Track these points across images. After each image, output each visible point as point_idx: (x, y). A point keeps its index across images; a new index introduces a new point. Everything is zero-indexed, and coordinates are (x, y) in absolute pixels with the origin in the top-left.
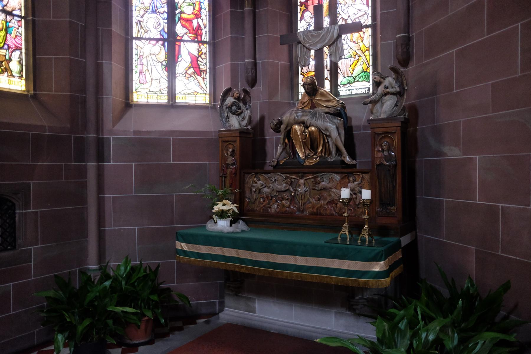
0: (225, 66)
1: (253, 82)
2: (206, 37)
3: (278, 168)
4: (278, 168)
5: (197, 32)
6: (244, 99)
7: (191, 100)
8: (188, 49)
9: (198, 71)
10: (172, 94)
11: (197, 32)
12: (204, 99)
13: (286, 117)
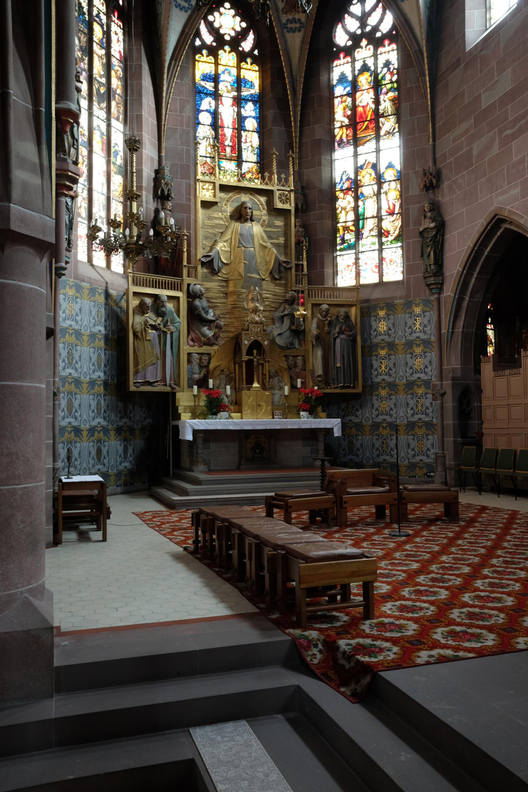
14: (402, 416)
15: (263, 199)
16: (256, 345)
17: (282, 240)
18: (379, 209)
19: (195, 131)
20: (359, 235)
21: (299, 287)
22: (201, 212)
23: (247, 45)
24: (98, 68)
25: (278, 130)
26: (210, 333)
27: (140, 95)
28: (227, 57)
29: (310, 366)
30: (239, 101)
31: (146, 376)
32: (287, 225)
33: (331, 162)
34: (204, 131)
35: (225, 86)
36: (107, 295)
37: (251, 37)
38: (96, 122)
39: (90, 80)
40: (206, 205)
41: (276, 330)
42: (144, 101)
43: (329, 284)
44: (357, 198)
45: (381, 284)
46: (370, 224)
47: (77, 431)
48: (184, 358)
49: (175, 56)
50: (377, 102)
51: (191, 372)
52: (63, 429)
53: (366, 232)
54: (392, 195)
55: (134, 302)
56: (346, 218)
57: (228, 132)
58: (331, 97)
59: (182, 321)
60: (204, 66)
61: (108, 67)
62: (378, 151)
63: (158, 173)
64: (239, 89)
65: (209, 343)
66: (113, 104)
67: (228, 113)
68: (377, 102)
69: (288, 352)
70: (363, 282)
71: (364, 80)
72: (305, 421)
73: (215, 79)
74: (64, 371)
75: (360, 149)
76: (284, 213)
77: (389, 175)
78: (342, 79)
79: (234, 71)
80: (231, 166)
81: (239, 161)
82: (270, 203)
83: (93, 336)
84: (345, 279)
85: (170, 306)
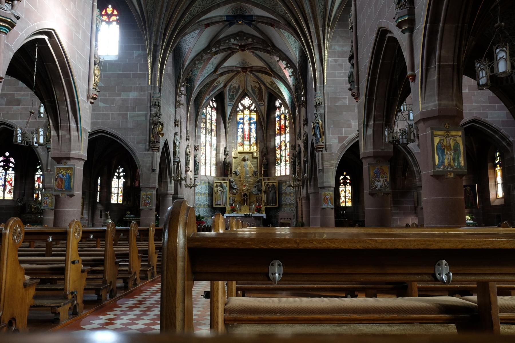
1: (24, 196)
2: (13, 185)
6: (22, 200)
7: (8, 198)
8: (8, 188)
10: (4, 197)
11: (11, 184)
12: (11, 198)
13: (31, 204)
15: (251, 155)
16: (245, 195)
17: (256, 165)
18: (285, 154)
19: (237, 134)
20: (281, 162)
21: (261, 178)
23: (252, 108)
24: (208, 125)
25: (260, 132)
26: (235, 191)
27: (220, 129)
28: (247, 112)
29: (263, 200)
30: (250, 124)
31: (218, 203)
32: (257, 161)
33: (274, 140)
34: (240, 134)
36: (209, 183)
37: (254, 105)
40: (235, 158)
41: (253, 190)
43: (273, 176)
44: (281, 150)
45: (286, 175)
46: (284, 158)
49: (229, 117)
50: (285, 123)
51: (230, 202)
53: (283, 160)
54: (288, 151)
55: (215, 185)
56: (278, 156)
58: (275, 121)
59: (228, 189)
60: (240, 115)
61: (211, 124)
62: (285, 137)
64: (250, 121)
65: (235, 194)
66: (213, 133)
68: (285, 123)
70: (282, 175)
71: (283, 116)
72: (256, 214)
73: (243, 119)
74: (196, 202)
75: (282, 136)
76: (256, 158)
78: (278, 116)
79: (249, 116)
81: (250, 141)
82: (253, 155)
85: (225, 185)
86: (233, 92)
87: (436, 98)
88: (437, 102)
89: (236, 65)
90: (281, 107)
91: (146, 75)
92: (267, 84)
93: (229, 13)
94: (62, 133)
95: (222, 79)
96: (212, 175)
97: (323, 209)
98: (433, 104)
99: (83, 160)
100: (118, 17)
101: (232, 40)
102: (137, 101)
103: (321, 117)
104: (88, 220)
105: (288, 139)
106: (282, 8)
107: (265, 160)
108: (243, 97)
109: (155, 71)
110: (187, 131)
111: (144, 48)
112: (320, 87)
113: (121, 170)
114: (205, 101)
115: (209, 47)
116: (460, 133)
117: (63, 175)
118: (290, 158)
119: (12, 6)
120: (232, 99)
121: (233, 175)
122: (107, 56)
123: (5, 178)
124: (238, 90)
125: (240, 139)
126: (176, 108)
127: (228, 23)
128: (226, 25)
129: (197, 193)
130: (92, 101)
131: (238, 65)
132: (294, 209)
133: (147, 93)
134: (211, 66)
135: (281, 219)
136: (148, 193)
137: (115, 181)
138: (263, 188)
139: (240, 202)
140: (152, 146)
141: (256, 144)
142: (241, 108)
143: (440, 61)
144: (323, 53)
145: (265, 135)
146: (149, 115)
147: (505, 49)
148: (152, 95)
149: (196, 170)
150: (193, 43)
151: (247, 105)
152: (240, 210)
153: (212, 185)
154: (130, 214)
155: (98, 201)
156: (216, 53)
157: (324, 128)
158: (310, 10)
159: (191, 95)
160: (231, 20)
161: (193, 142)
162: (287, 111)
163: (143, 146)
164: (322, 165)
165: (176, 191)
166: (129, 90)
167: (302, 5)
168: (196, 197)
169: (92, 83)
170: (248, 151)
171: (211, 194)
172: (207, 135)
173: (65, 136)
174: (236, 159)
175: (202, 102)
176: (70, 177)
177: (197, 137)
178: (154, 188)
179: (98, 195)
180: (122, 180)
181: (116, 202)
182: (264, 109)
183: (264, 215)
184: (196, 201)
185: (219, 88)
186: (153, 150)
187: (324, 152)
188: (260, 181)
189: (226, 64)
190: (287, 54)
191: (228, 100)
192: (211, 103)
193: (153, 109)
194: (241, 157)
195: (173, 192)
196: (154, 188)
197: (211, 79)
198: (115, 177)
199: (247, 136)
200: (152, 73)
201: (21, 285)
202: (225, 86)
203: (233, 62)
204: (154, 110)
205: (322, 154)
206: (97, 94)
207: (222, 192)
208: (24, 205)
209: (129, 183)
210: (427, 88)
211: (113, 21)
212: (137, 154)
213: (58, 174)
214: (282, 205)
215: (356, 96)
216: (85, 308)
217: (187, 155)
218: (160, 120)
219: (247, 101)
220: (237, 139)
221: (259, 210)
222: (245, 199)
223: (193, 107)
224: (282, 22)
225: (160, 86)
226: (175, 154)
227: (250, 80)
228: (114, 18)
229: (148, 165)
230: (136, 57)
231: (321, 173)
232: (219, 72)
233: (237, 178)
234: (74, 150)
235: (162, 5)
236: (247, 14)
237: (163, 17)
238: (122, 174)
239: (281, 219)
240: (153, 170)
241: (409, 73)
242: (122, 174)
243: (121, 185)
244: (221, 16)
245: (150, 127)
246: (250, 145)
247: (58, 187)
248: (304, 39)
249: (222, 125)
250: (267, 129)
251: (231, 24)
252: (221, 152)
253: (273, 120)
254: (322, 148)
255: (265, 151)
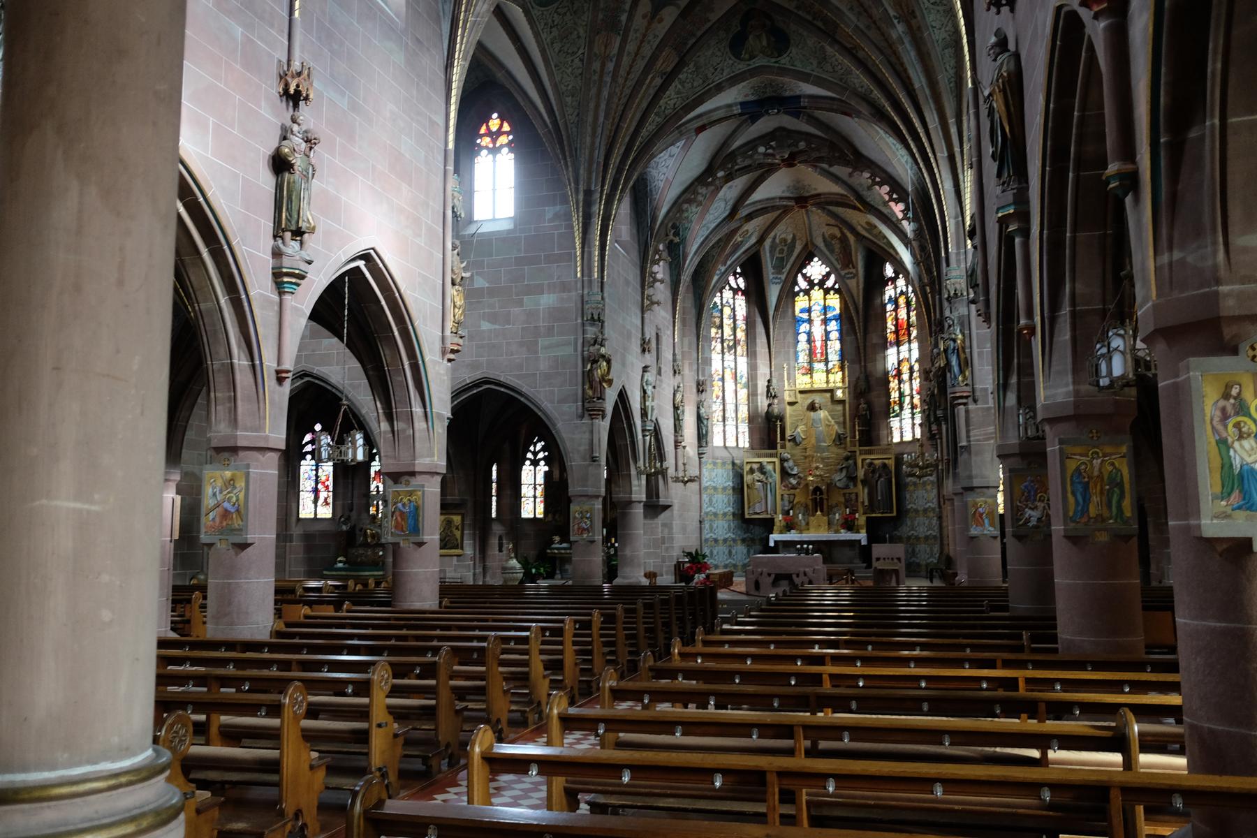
0: (339, 503)
1: (351, 510)
2: (331, 488)
3: (361, 545)
4: (361, 545)
5: (327, 487)
8: (323, 495)
9: (327, 504)
11: (327, 487)
12: (330, 516)
14: (922, 531)
15: (828, 395)
16: (817, 489)
17: (841, 419)
18: (912, 390)
20: (901, 408)
21: (853, 449)
22: (788, 408)
24: (728, 331)
26: (794, 481)
28: (817, 294)
29: (860, 500)
30: (825, 322)
31: (756, 509)
33: (885, 358)
34: (803, 345)
35: (817, 316)
36: (733, 464)
37: (833, 278)
38: (726, 364)
39: (722, 342)
40: (791, 404)
41: (837, 477)
42: (758, 341)
44: (900, 382)
46: (907, 399)
47: (716, 541)
48: (778, 497)
49: (776, 309)
50: (909, 317)
51: (783, 506)
52: (707, 540)
54: (916, 384)
55: (747, 468)
56: (895, 395)
57: (818, 344)
59: (777, 476)
60: (801, 302)
61: (734, 329)
62: (910, 350)
63: (769, 381)
66: (739, 348)
67: (818, 331)
68: (909, 317)
69: (848, 491)
70: (905, 439)
71: (902, 300)
72: (845, 535)
73: (809, 310)
74: (706, 508)
76: (842, 402)
77: (916, 367)
80: (821, 366)
81: (827, 361)
82: (832, 397)
83: (724, 489)
84: (896, 439)
85: (770, 467)
86: (782, 251)
87: (1070, 379)
88: (1071, 388)
89: (779, 194)
90: (897, 277)
91: (571, 257)
92: (859, 229)
93: (747, 95)
94: (399, 425)
95: (753, 227)
96: (741, 445)
97: (972, 538)
98: (1064, 390)
99: (438, 474)
100: (511, 137)
101: (762, 149)
102: (556, 314)
103: (962, 325)
104: (474, 558)
105: (915, 354)
106: (860, 80)
107: (863, 406)
108: (807, 259)
109: (589, 247)
110: (674, 355)
111: (565, 201)
112: (958, 254)
113: (539, 446)
114: (716, 278)
115: (709, 171)
116: (1124, 449)
117: (404, 505)
118: (922, 401)
119: (301, 243)
120: (779, 268)
121: (788, 444)
122: (494, 220)
123: (317, 476)
124: (792, 247)
125: (803, 358)
126: (643, 312)
127: (743, 118)
128: (746, 120)
129: (706, 488)
130: (452, 356)
131: (787, 194)
132: (935, 521)
133: (574, 295)
134: (722, 204)
135: (878, 559)
136: (586, 507)
137: (527, 469)
138: (861, 473)
139: (806, 506)
140: (590, 410)
141: (842, 368)
142: (803, 284)
143: (1073, 303)
144: (961, 177)
145: (861, 345)
146: (580, 341)
147: (1122, 332)
148: (586, 299)
149: (702, 437)
150: (673, 168)
151: (816, 278)
152: (807, 524)
153: (741, 468)
154: (561, 542)
155: (494, 515)
156: (729, 178)
157: (968, 351)
158: (923, 80)
159: (679, 275)
160: (751, 110)
161: (694, 374)
162: (910, 289)
163: (574, 407)
164: (968, 437)
165: (652, 491)
166: (539, 290)
167: (905, 70)
168: (704, 497)
169: (450, 324)
170: (824, 386)
171: (739, 488)
172: (727, 355)
173: (404, 431)
174: (794, 407)
175: (708, 282)
176: (417, 508)
177: (703, 363)
178: (597, 497)
179: (494, 504)
180: (543, 468)
181: (532, 516)
182: (857, 285)
183: (862, 536)
184: (704, 506)
185: (747, 246)
186: (592, 417)
187: (971, 407)
188: (851, 457)
189: (759, 194)
190: (890, 170)
191: (771, 270)
192: (731, 279)
193: (589, 328)
194: (805, 401)
195: (643, 497)
196: (597, 497)
197: (725, 230)
198: (528, 463)
199: (819, 350)
200: (583, 253)
201: (307, 767)
202: (761, 240)
203: (774, 187)
204: (591, 332)
205: (967, 412)
206: (461, 341)
207: (765, 484)
208: (353, 528)
209: (556, 474)
210: (1054, 357)
211: (502, 146)
212: (560, 425)
213: (395, 503)
214: (908, 511)
215: (987, 320)
216: (403, 787)
217: (676, 408)
218: (603, 351)
219: (816, 269)
220: (796, 359)
221: (849, 525)
222: (819, 500)
223: (690, 295)
224: (864, 109)
225: (602, 277)
226: (644, 414)
227: (819, 223)
228: (503, 140)
229: (582, 448)
230: (551, 220)
231: (965, 456)
232: (743, 212)
233: (797, 451)
234: (422, 456)
235: (597, 106)
236: (787, 94)
237: (599, 130)
238: (541, 455)
239: (878, 559)
240: (594, 459)
241: (1023, 322)
242: (541, 455)
243: (540, 479)
244: (729, 106)
245: (584, 366)
246: (828, 372)
247: (396, 527)
248: (917, 146)
249: (760, 329)
250: (866, 332)
251: (754, 118)
252: (759, 391)
253: (879, 311)
254: (967, 397)
255: (862, 385)
